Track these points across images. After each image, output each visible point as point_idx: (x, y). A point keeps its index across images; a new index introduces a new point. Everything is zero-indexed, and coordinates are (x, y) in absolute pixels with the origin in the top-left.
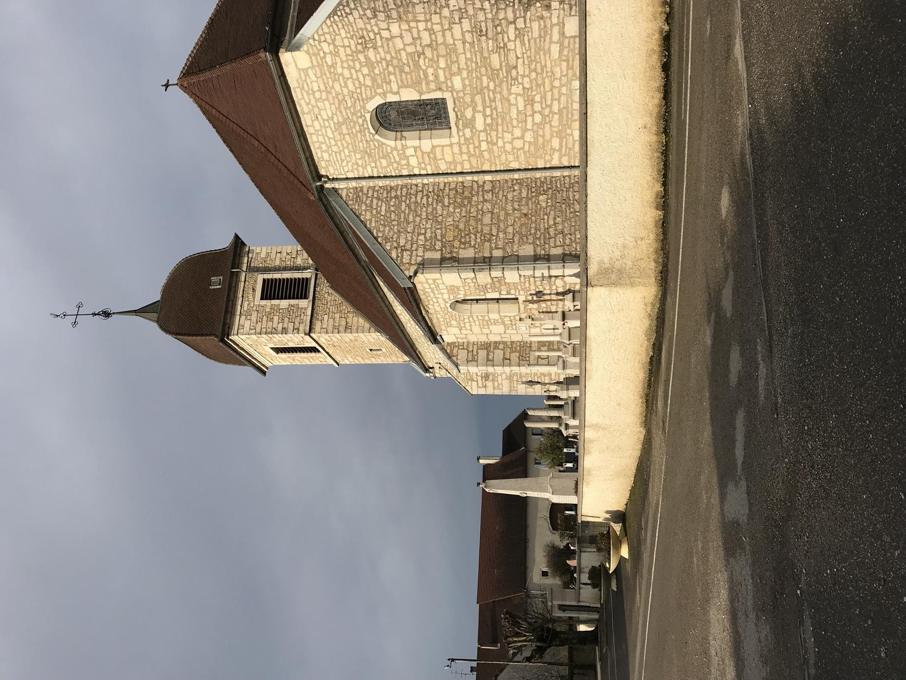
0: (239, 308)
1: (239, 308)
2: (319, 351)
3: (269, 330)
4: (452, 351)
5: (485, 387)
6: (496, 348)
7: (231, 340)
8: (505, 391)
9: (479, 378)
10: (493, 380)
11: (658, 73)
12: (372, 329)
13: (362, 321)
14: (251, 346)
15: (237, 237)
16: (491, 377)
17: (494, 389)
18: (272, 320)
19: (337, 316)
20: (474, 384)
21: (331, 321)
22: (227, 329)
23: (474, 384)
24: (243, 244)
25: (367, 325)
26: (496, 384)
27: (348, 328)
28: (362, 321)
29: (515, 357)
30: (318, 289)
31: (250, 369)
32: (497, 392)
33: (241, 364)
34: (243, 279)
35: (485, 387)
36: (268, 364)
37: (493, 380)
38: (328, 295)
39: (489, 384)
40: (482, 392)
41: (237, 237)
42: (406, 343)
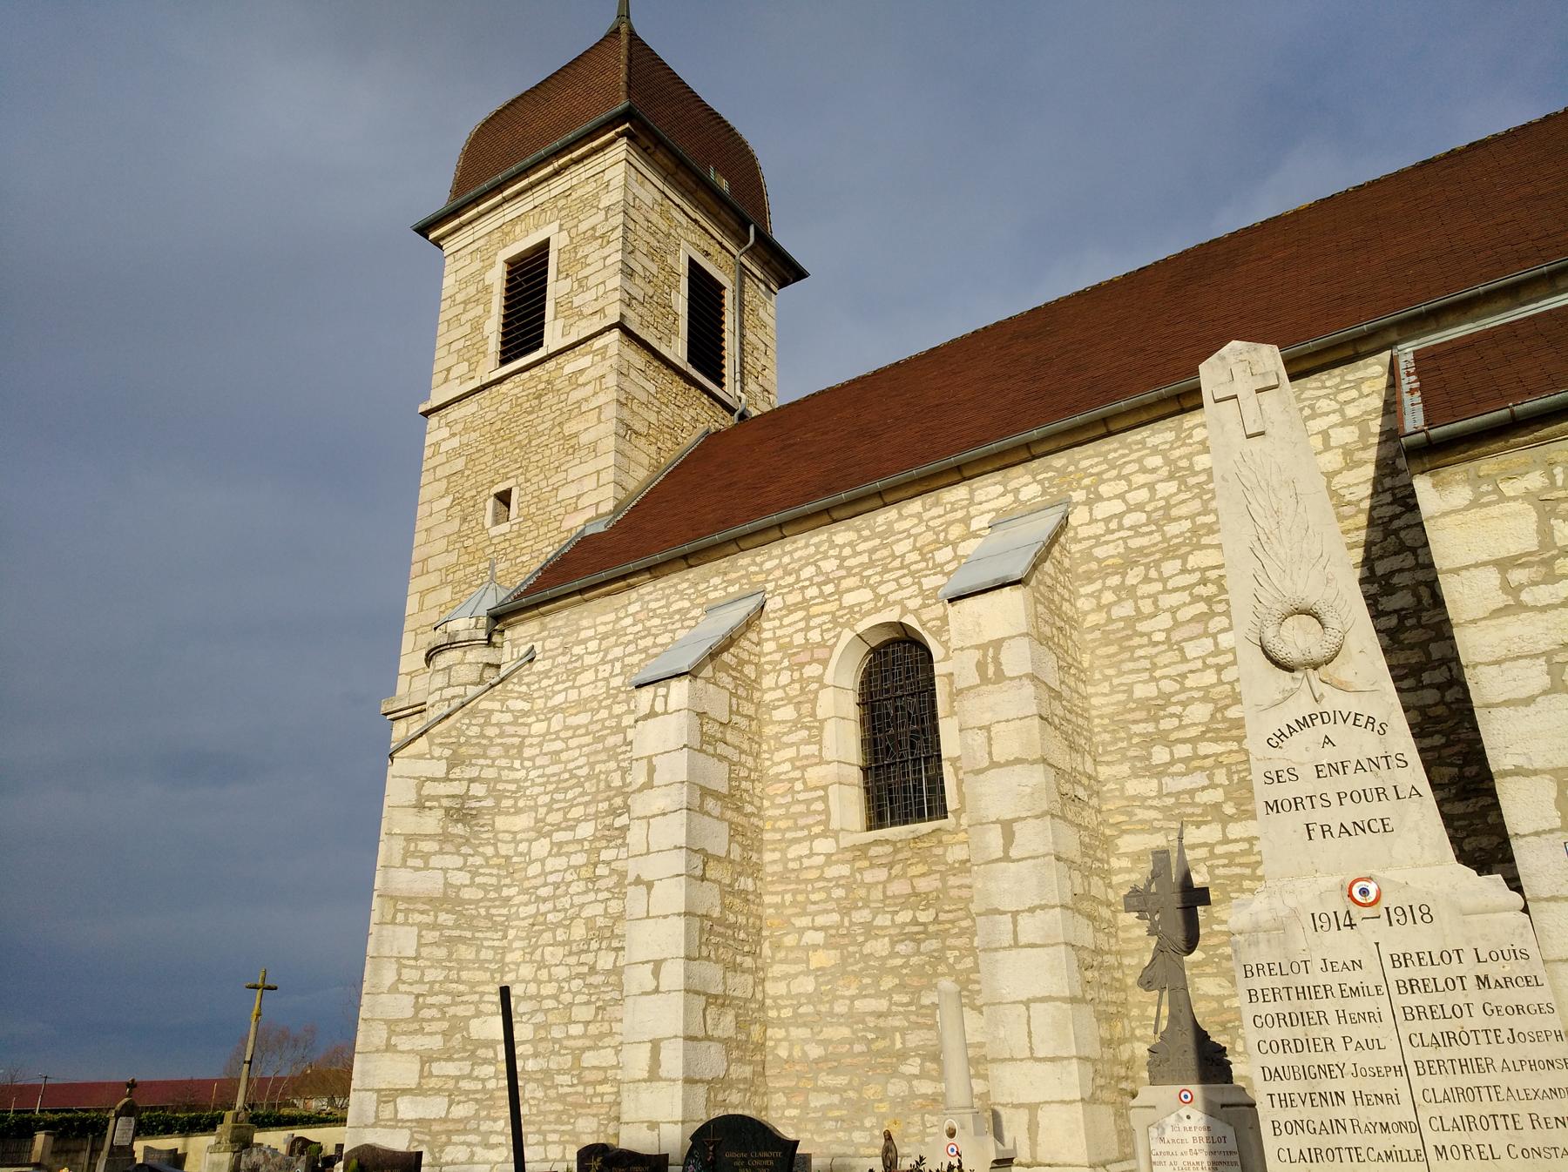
2: (503, 362)
3: (631, 236)
4: (726, 667)
5: (420, 806)
6: (736, 831)
7: (612, 142)
9: (457, 788)
10: (444, 837)
12: (622, 495)
13: (641, 474)
14: (566, 194)
15: (800, 274)
16: (459, 829)
17: (409, 838)
19: (653, 418)
20: (439, 769)
21: (643, 397)
22: (646, 142)
23: (439, 769)
24: (783, 284)
25: (632, 485)
26: (426, 846)
27: (627, 431)
28: (640, 476)
31: (439, 201)
32: (388, 850)
33: (460, 185)
34: (726, 243)
35: (420, 806)
36: (450, 246)
37: (444, 837)
38: (695, 420)
39: (431, 822)
40: (397, 791)
41: (800, 274)
42: (748, 527)
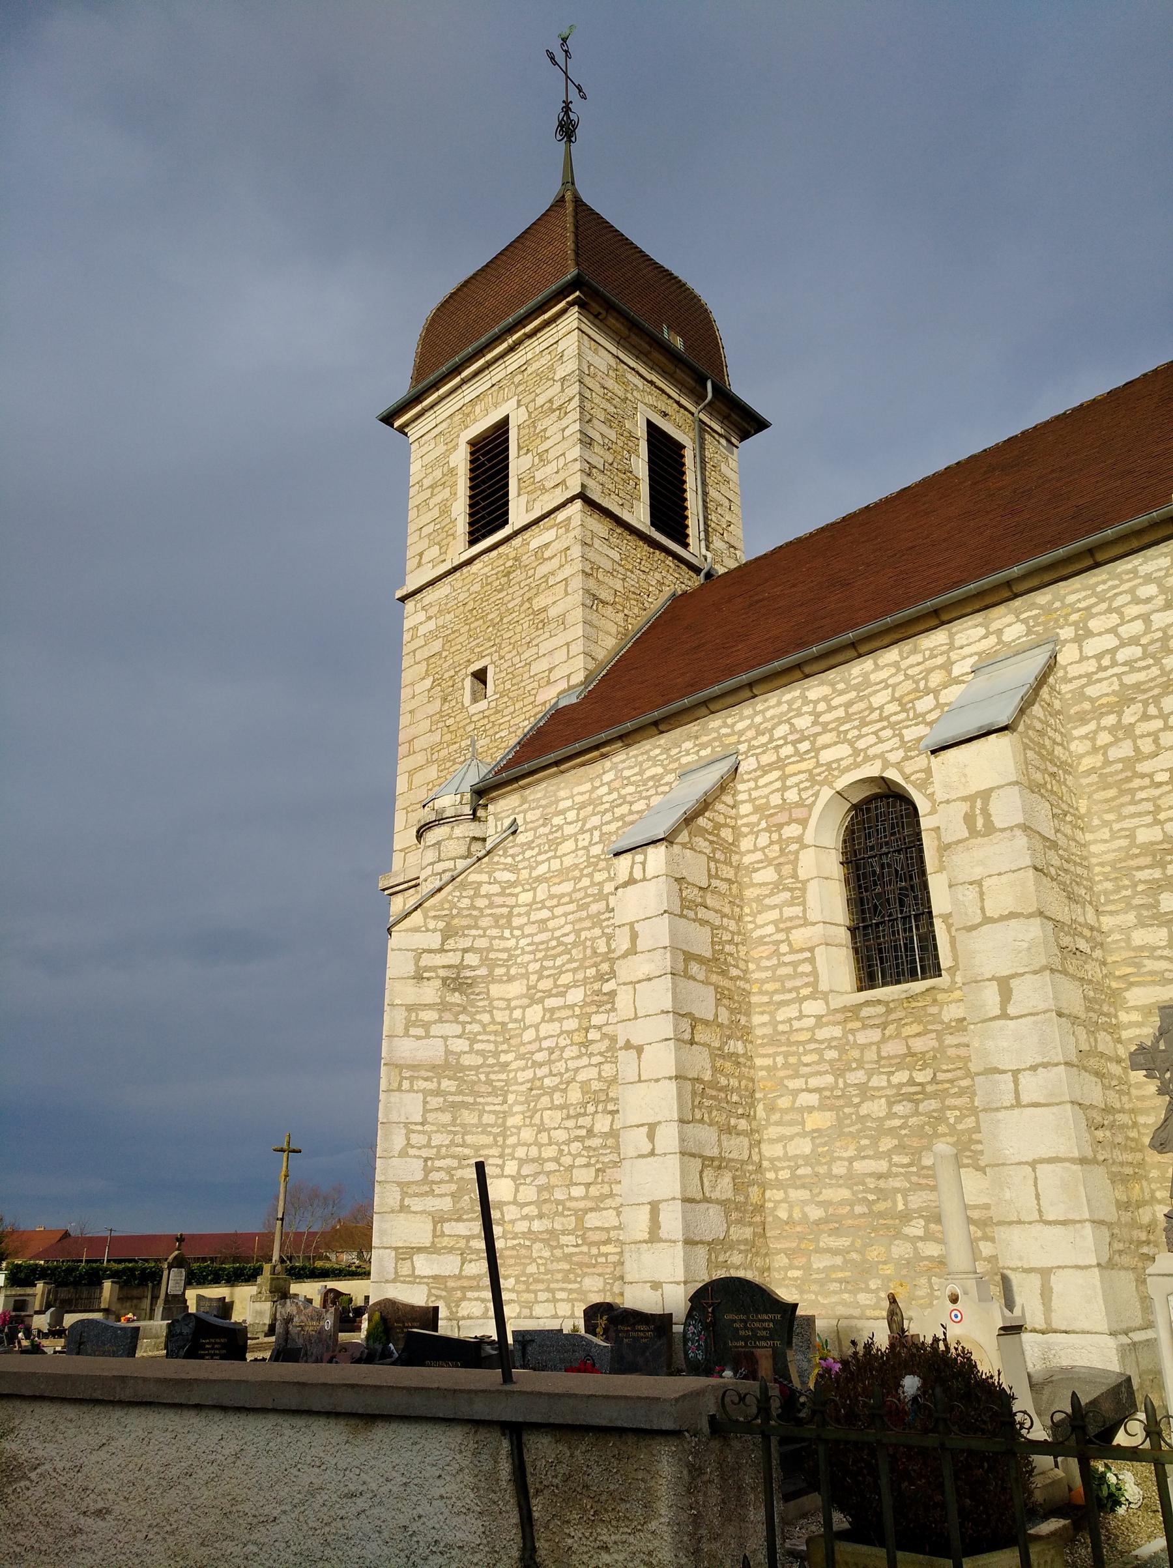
0: (632, 364)
1: (632, 364)
2: (472, 543)
3: (588, 405)
4: (703, 832)
5: (419, 977)
6: (722, 995)
7: (564, 311)
8: (401, 1045)
9: (452, 959)
10: (443, 1007)
11: (381, 1433)
12: (592, 665)
13: (610, 643)
14: (521, 370)
15: (761, 425)
16: (456, 998)
17: (410, 1008)
18: (607, 422)
19: (618, 585)
20: (435, 941)
21: (609, 567)
22: (596, 308)
23: (435, 941)
24: (744, 436)
25: (601, 655)
26: (428, 1015)
27: (593, 600)
28: (608, 645)
29: (700, 1063)
30: (669, 561)
31: (402, 389)
32: (393, 1020)
33: (420, 371)
34: (683, 402)
35: (419, 977)
36: (414, 432)
37: (443, 1007)
38: (660, 583)
39: (430, 992)
40: (398, 964)
41: (761, 425)
42: (716, 689)
